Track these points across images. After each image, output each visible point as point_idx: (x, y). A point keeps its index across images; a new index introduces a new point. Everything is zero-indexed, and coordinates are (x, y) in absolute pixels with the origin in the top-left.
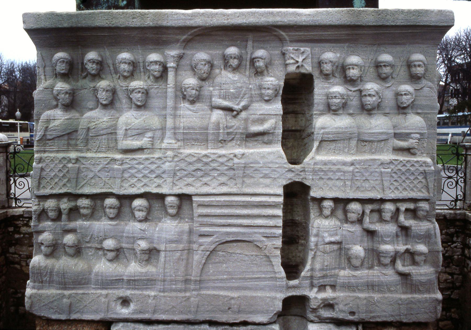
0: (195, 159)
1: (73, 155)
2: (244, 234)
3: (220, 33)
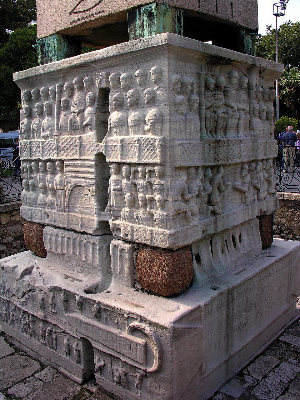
0: (64, 141)
1: (29, 141)
2: (81, 182)
3: (72, 70)
